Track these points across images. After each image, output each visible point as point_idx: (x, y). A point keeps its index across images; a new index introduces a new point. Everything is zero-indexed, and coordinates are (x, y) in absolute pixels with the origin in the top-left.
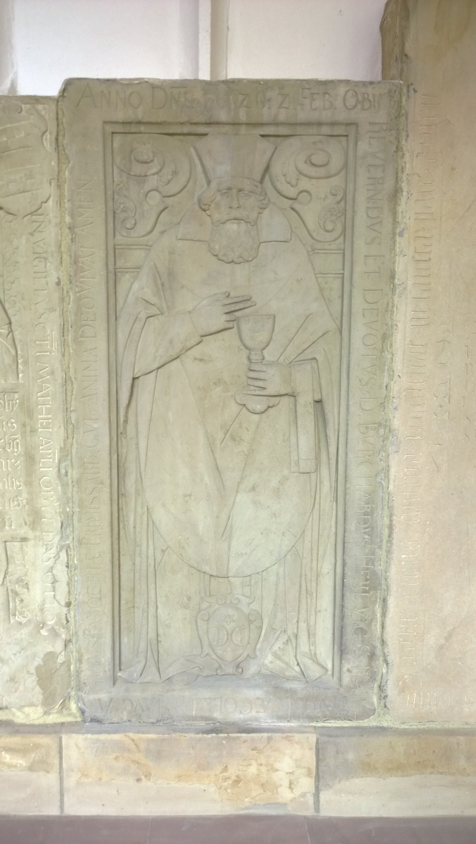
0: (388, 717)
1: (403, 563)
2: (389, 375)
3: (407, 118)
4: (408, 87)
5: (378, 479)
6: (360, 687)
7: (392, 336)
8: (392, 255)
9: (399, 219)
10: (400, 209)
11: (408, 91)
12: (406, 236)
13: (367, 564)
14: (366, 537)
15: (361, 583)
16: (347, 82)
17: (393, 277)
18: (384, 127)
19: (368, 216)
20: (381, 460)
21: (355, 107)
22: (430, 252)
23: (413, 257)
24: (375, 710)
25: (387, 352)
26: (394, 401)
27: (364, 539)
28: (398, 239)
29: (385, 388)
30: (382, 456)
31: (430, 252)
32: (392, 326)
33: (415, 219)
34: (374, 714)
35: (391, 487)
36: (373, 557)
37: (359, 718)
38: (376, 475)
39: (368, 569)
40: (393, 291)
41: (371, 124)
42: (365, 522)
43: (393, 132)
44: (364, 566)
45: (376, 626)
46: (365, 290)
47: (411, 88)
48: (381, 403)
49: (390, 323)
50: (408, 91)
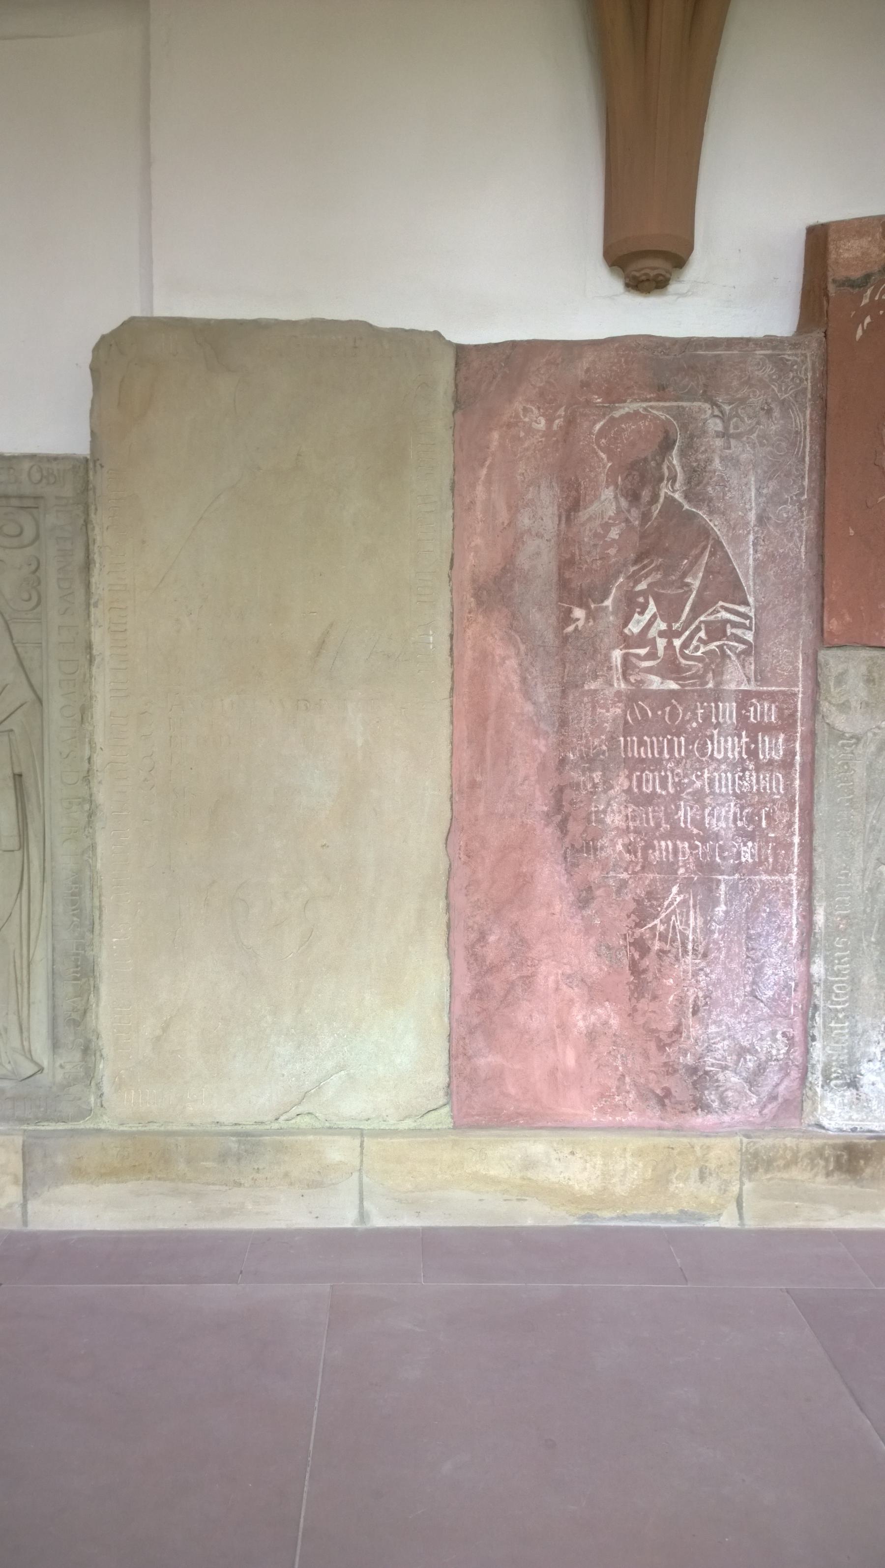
0: (105, 1118)
1: (114, 947)
2: (91, 747)
3: (95, 493)
4: (95, 462)
5: (85, 857)
6: (74, 1085)
7: (91, 707)
8: (87, 626)
9: (93, 589)
10: (93, 580)
11: (95, 466)
12: (100, 606)
13: (77, 949)
14: (75, 919)
15: (72, 970)
16: (33, 457)
17: (89, 647)
18: (71, 501)
19: (59, 587)
20: (87, 837)
21: (40, 481)
22: (125, 623)
23: (109, 628)
24: (91, 1110)
25: (87, 724)
26: (99, 774)
27: (73, 922)
28: (92, 609)
29: (87, 761)
30: (89, 833)
31: (125, 623)
32: (91, 698)
33: (109, 590)
34: (89, 1115)
35: (99, 865)
36: (82, 941)
37: (75, 1119)
38: (83, 853)
39: (78, 954)
40: (91, 662)
41: (57, 498)
42: (73, 903)
43: (80, 506)
44: (75, 951)
45: (91, 1017)
46: (60, 660)
47: (98, 463)
48: (84, 777)
49: (89, 694)
50: (95, 466)
